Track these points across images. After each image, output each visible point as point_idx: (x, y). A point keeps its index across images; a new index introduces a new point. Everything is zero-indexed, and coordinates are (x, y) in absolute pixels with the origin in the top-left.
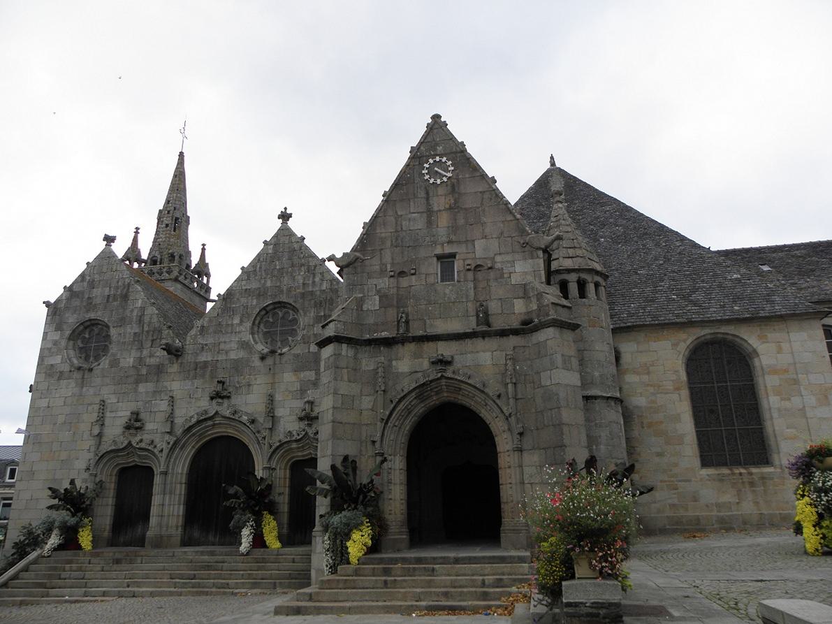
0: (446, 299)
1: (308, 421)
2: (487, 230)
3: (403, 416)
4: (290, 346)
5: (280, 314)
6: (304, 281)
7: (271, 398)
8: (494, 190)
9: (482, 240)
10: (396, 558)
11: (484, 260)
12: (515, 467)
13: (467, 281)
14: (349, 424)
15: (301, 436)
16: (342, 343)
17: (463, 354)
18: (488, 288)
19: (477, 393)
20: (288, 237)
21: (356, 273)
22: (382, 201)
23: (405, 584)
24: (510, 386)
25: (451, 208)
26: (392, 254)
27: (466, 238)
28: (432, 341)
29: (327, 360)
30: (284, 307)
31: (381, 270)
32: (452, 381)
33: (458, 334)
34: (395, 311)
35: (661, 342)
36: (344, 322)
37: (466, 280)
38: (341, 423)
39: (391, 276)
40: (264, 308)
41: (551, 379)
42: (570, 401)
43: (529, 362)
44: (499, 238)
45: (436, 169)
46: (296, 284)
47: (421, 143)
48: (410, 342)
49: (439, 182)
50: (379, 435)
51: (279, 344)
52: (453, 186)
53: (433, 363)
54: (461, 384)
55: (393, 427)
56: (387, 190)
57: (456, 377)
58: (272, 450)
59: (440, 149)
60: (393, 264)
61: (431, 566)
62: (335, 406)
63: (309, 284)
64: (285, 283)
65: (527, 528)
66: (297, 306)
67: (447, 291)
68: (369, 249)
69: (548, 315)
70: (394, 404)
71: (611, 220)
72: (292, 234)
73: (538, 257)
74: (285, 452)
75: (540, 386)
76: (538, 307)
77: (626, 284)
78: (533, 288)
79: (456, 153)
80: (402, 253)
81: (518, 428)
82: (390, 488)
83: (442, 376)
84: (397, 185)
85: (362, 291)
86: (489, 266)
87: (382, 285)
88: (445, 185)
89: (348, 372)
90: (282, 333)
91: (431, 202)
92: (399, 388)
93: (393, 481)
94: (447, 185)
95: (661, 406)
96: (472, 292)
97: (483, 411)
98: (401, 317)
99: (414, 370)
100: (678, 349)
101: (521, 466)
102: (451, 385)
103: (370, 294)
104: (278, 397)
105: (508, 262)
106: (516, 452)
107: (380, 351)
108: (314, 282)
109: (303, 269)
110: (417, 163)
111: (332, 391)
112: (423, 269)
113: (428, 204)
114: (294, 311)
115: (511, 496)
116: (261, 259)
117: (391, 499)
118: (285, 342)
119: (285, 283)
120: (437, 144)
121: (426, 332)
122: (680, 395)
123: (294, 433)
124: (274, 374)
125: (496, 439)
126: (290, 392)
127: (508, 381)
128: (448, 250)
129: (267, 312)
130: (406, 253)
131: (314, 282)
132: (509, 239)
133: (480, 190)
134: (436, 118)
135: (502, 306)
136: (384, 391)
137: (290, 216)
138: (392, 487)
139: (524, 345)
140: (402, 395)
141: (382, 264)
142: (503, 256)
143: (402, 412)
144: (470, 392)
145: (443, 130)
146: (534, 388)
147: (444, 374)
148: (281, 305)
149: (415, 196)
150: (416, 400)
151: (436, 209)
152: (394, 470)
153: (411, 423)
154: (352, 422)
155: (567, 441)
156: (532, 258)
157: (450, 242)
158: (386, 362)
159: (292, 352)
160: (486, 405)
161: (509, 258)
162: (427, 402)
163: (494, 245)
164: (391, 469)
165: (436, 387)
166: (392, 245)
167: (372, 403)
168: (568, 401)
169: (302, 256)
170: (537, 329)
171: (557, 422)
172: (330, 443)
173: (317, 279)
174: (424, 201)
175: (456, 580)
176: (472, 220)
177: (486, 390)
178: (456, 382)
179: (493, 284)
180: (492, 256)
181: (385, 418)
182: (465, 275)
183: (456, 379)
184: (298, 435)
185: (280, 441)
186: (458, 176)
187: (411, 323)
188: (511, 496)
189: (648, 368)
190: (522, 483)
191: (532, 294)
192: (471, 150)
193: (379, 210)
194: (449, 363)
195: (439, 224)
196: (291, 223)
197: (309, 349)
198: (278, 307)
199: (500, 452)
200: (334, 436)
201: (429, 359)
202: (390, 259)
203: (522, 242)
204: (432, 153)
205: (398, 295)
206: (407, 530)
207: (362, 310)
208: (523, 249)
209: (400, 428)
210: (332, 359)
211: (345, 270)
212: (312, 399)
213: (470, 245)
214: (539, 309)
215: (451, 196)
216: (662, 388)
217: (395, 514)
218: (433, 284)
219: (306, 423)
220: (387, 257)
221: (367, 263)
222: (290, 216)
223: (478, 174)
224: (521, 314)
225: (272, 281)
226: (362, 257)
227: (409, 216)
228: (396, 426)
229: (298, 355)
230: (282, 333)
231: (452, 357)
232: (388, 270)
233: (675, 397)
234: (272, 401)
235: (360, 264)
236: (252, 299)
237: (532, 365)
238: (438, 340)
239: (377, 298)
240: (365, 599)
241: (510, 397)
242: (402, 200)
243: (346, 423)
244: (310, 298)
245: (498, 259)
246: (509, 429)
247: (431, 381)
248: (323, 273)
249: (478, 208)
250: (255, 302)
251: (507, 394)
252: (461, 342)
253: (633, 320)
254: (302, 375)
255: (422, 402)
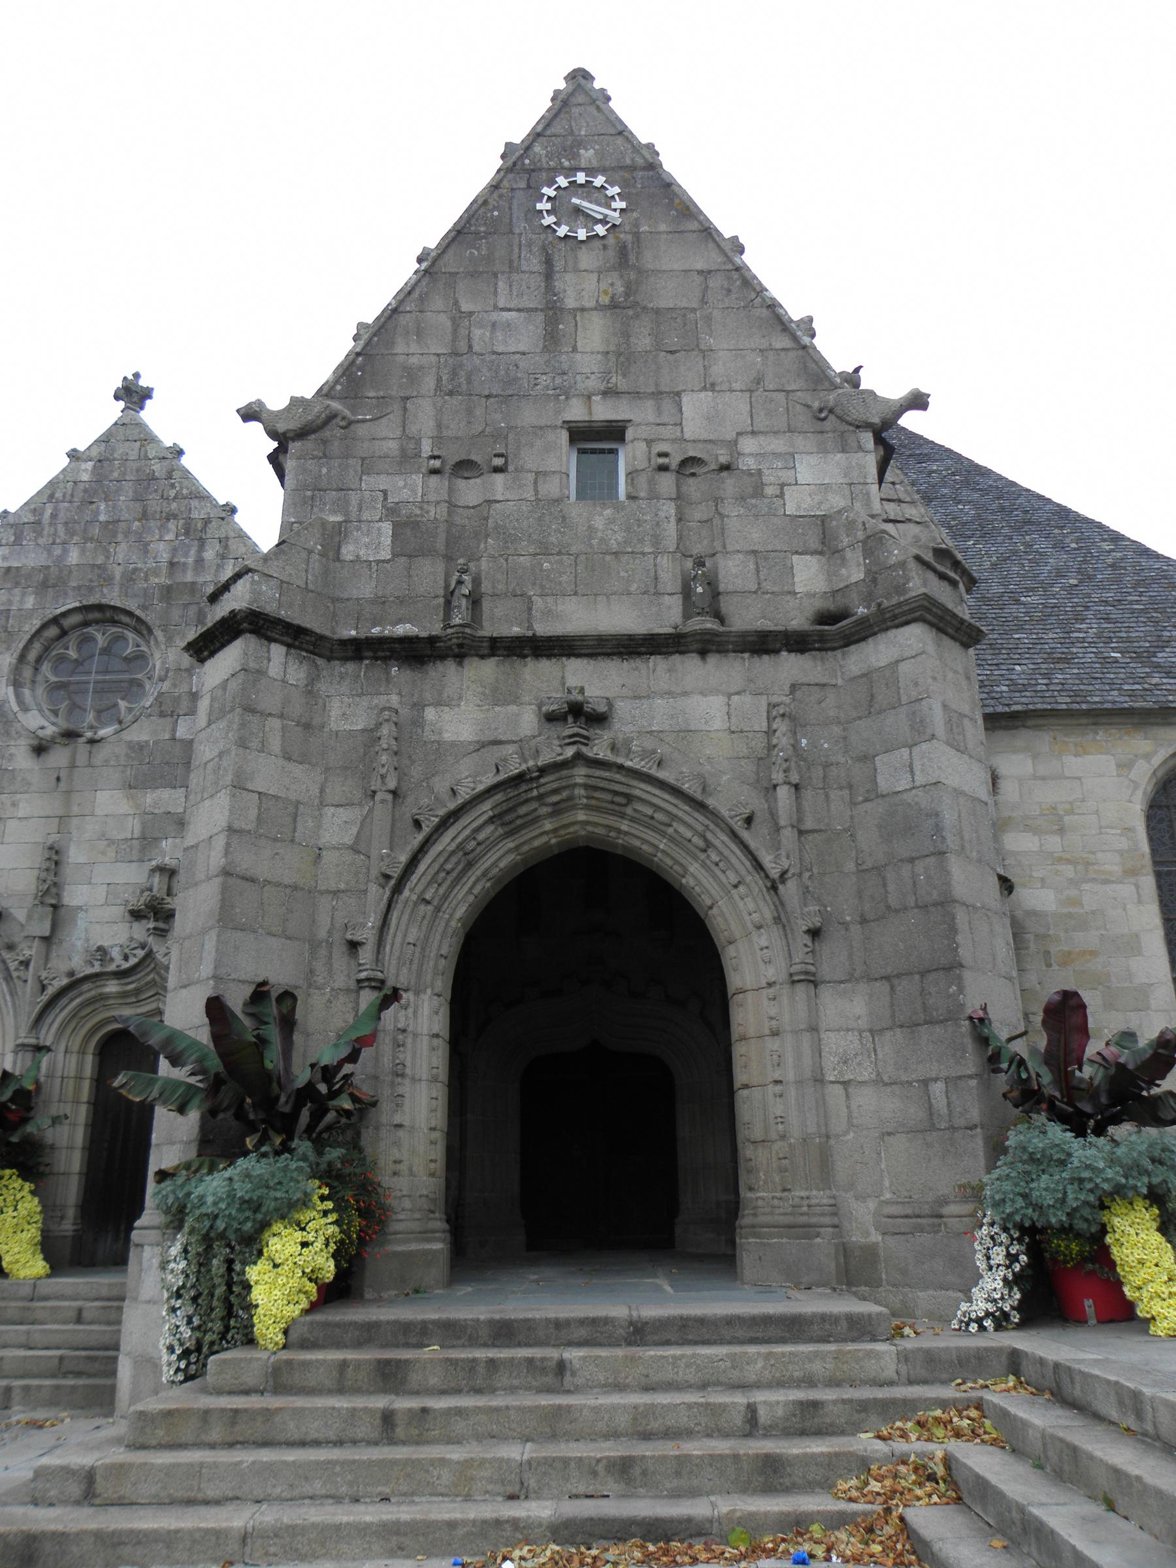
0: (595, 542)
1: (156, 920)
2: (718, 370)
3: (448, 873)
4: (120, 722)
5: (101, 640)
6: (174, 556)
7: (55, 858)
8: (738, 269)
9: (703, 395)
10: (424, 1323)
11: (709, 446)
12: (795, 1032)
13: (658, 498)
14: (278, 885)
15: (133, 961)
16: (271, 640)
17: (640, 698)
18: (717, 521)
19: (682, 810)
20: (138, 443)
21: (325, 456)
22: (416, 273)
23: (460, 1426)
24: (783, 792)
25: (614, 306)
26: (439, 411)
27: (657, 385)
28: (549, 656)
29: (219, 692)
30: (114, 622)
31: (403, 450)
32: (607, 774)
33: (631, 637)
34: (440, 567)
35: (1090, 757)
36: (282, 582)
37: (654, 496)
38: (253, 880)
39: (435, 472)
40: (55, 620)
41: (912, 772)
42: (967, 837)
43: (836, 730)
44: (751, 391)
45: (575, 201)
46: (151, 564)
47: (536, 135)
48: (482, 657)
49: (582, 234)
50: (372, 921)
51: (90, 717)
52: (623, 251)
53: (551, 718)
54: (635, 783)
55: (416, 904)
56: (433, 245)
57: (620, 760)
58: (45, 998)
59: (587, 155)
60: (438, 440)
61: (553, 1353)
62: (236, 825)
63: (185, 564)
64: (120, 558)
65: (835, 1221)
66: (149, 618)
67: (599, 522)
68: (371, 394)
69: (901, 589)
70: (426, 830)
71: (945, 491)
72: (147, 438)
73: (860, 448)
74: (83, 1006)
75: (874, 794)
76: (868, 572)
77: (995, 622)
78: (850, 525)
79: (633, 168)
80: (470, 412)
81: (805, 916)
82: (400, 1090)
83: (578, 756)
84: (460, 234)
85: (342, 506)
86: (723, 460)
87: (405, 494)
88: (597, 244)
89: (284, 728)
90: (102, 689)
91: (558, 285)
92: (441, 785)
93: (408, 1071)
94: (605, 247)
95: (1093, 912)
96: (671, 529)
97: (694, 867)
98: (460, 582)
99: (489, 736)
100: (1132, 776)
101: (814, 1029)
102: (602, 784)
103: (366, 516)
104: (75, 855)
105: (776, 455)
106: (801, 989)
107: (388, 680)
108: (200, 561)
109: (172, 525)
110: (523, 185)
111: (228, 779)
112: (530, 459)
113: (549, 289)
114: (139, 633)
115: (781, 1120)
116: (59, 495)
117: (399, 1126)
118: (107, 713)
119: (120, 558)
120: (580, 143)
121: (530, 627)
122: (1137, 887)
123: (116, 953)
124: (69, 792)
125: (730, 956)
126: (111, 842)
127: (778, 776)
128: (603, 412)
129: (64, 633)
130: (478, 412)
131: (200, 561)
132: (781, 397)
133: (699, 266)
134: (579, 77)
135: (758, 571)
136: (394, 793)
137: (147, 394)
138: (405, 1088)
139: (824, 681)
140: (452, 806)
141: (405, 436)
142: (761, 438)
143: (446, 861)
144: (657, 808)
145: (598, 108)
146: (853, 804)
147: (584, 749)
148: (104, 614)
149: (513, 267)
150: (490, 828)
151: (570, 303)
152: (415, 1035)
153: (471, 898)
154: (287, 881)
155: (965, 954)
156: (843, 451)
157: (609, 393)
158: (405, 712)
159: (127, 736)
160: (709, 844)
161: (778, 444)
162: (526, 835)
163: (736, 410)
164: (404, 1031)
165: (556, 791)
166: (438, 387)
167: (354, 830)
168: (962, 838)
169: (172, 493)
170: (864, 631)
171: (935, 893)
172: (211, 942)
173: (209, 554)
174: (537, 282)
175: (651, 1408)
176: (673, 341)
177: (711, 802)
178: (618, 777)
179: (732, 510)
180: (730, 436)
181: (395, 873)
182: (651, 482)
183: (621, 767)
184: (126, 958)
185: (71, 974)
186: (637, 225)
187: (486, 604)
188: (781, 1120)
189: (1061, 819)
190: (819, 1080)
191: (846, 541)
192: (672, 164)
193: (406, 294)
194: (599, 719)
195: (579, 344)
196: (151, 415)
197: (174, 730)
198: (97, 622)
199: (742, 991)
200: (226, 918)
201: (540, 707)
202: (432, 423)
203: (816, 405)
204: (566, 164)
205: (449, 523)
206: (446, 1226)
207: (338, 559)
208: (819, 426)
209: (438, 909)
210: (233, 685)
211: (294, 447)
212: (174, 863)
213: (668, 405)
214: (872, 577)
215: (615, 274)
216: (1096, 867)
217: (412, 1173)
218: (558, 501)
219: (151, 925)
220: (424, 420)
221: (361, 430)
222: (147, 394)
223: (694, 226)
224: (814, 595)
225: (83, 551)
226: (347, 413)
227: (495, 316)
228: (428, 902)
229: (141, 747)
230: (102, 689)
231: (610, 705)
232: (424, 455)
233: (1126, 890)
234: (56, 863)
235: (339, 433)
236: (23, 595)
237: (845, 738)
238: (569, 656)
239: (387, 528)
240: (308, 1489)
241: (782, 823)
242: (473, 275)
243: (267, 882)
244: (186, 598)
245: (748, 445)
246: (777, 920)
247: (543, 771)
248: (227, 538)
249: (694, 310)
250: (30, 602)
251: (773, 814)
252: (638, 663)
253: (1023, 700)
254: (150, 798)
255: (509, 834)
